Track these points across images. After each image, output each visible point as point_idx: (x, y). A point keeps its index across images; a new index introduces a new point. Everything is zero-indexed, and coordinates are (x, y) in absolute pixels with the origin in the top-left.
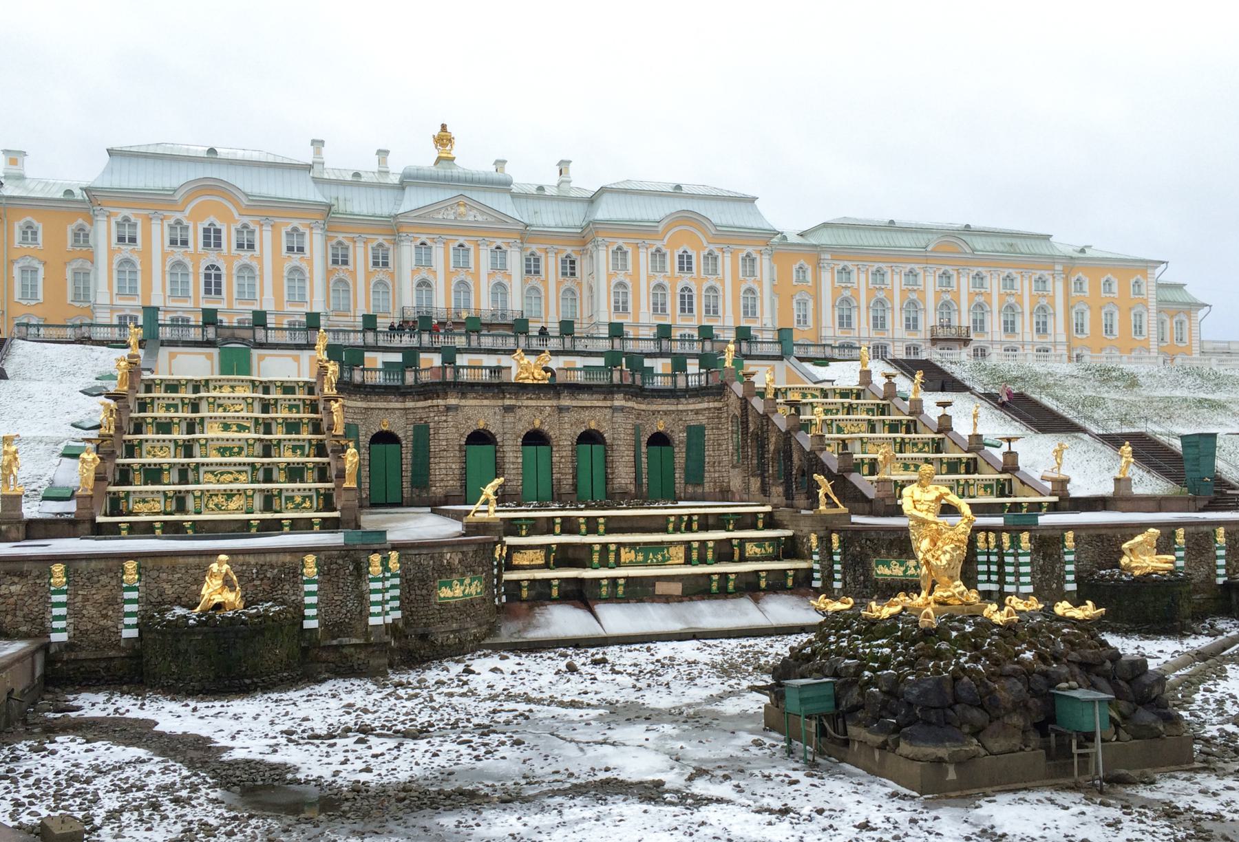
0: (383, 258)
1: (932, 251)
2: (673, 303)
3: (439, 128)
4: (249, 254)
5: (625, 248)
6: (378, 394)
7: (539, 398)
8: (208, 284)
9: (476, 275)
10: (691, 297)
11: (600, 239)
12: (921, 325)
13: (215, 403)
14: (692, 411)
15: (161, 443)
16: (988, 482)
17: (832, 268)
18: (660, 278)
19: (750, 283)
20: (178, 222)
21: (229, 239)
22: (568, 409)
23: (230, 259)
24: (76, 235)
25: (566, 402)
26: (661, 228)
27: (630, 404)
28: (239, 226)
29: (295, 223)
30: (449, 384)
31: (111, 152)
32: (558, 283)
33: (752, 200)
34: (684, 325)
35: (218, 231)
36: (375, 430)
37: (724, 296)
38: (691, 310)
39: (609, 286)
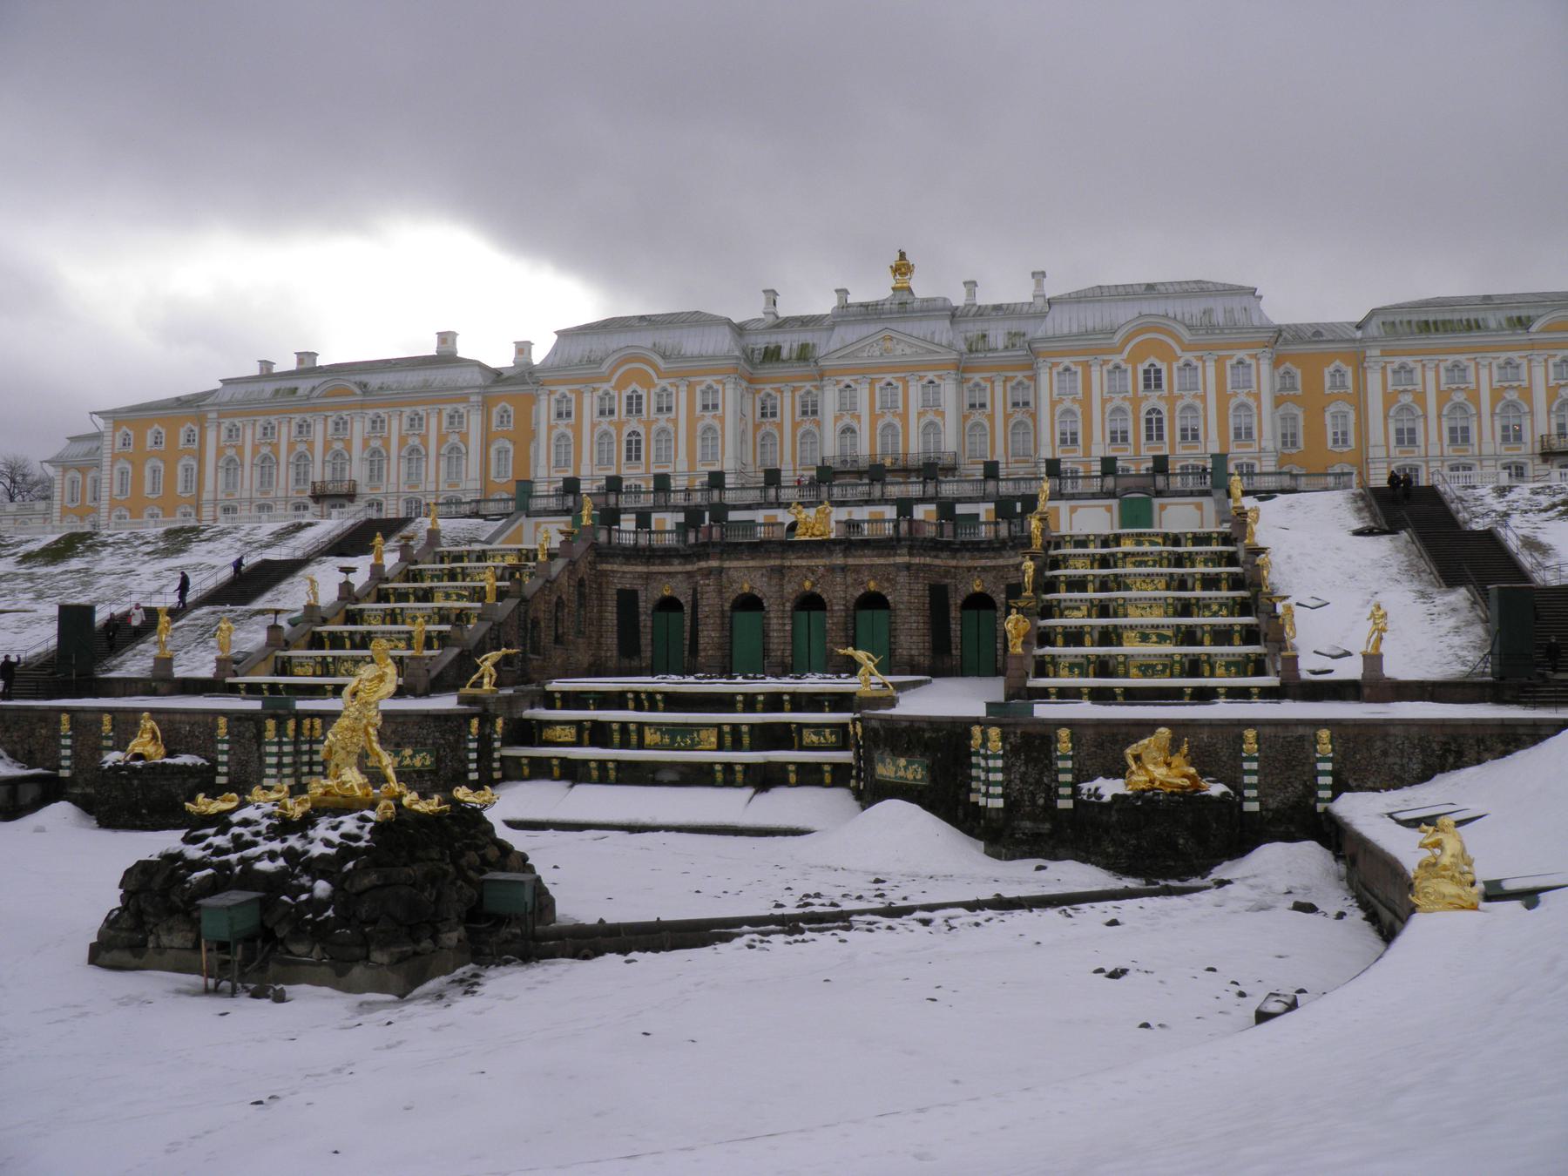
0: (812, 406)
1: (1537, 332)
2: (1136, 429)
3: (898, 259)
5: (1073, 368)
6: (660, 557)
7: (812, 557)
8: (629, 450)
9: (905, 417)
10: (1160, 421)
11: (1041, 360)
12: (1527, 436)
14: (1013, 566)
15: (374, 613)
16: (1231, 659)
17: (1384, 368)
18: (1117, 401)
19: (1242, 397)
20: (607, 393)
22: (844, 569)
23: (648, 424)
25: (839, 560)
26: (1117, 338)
27: (916, 560)
28: (658, 390)
29: (709, 380)
30: (714, 545)
31: (556, 332)
32: (1007, 417)
33: (1253, 291)
34: (637, 475)
35: (639, 397)
36: (657, 595)
37: (1206, 416)
38: (1160, 437)
39: (1052, 415)
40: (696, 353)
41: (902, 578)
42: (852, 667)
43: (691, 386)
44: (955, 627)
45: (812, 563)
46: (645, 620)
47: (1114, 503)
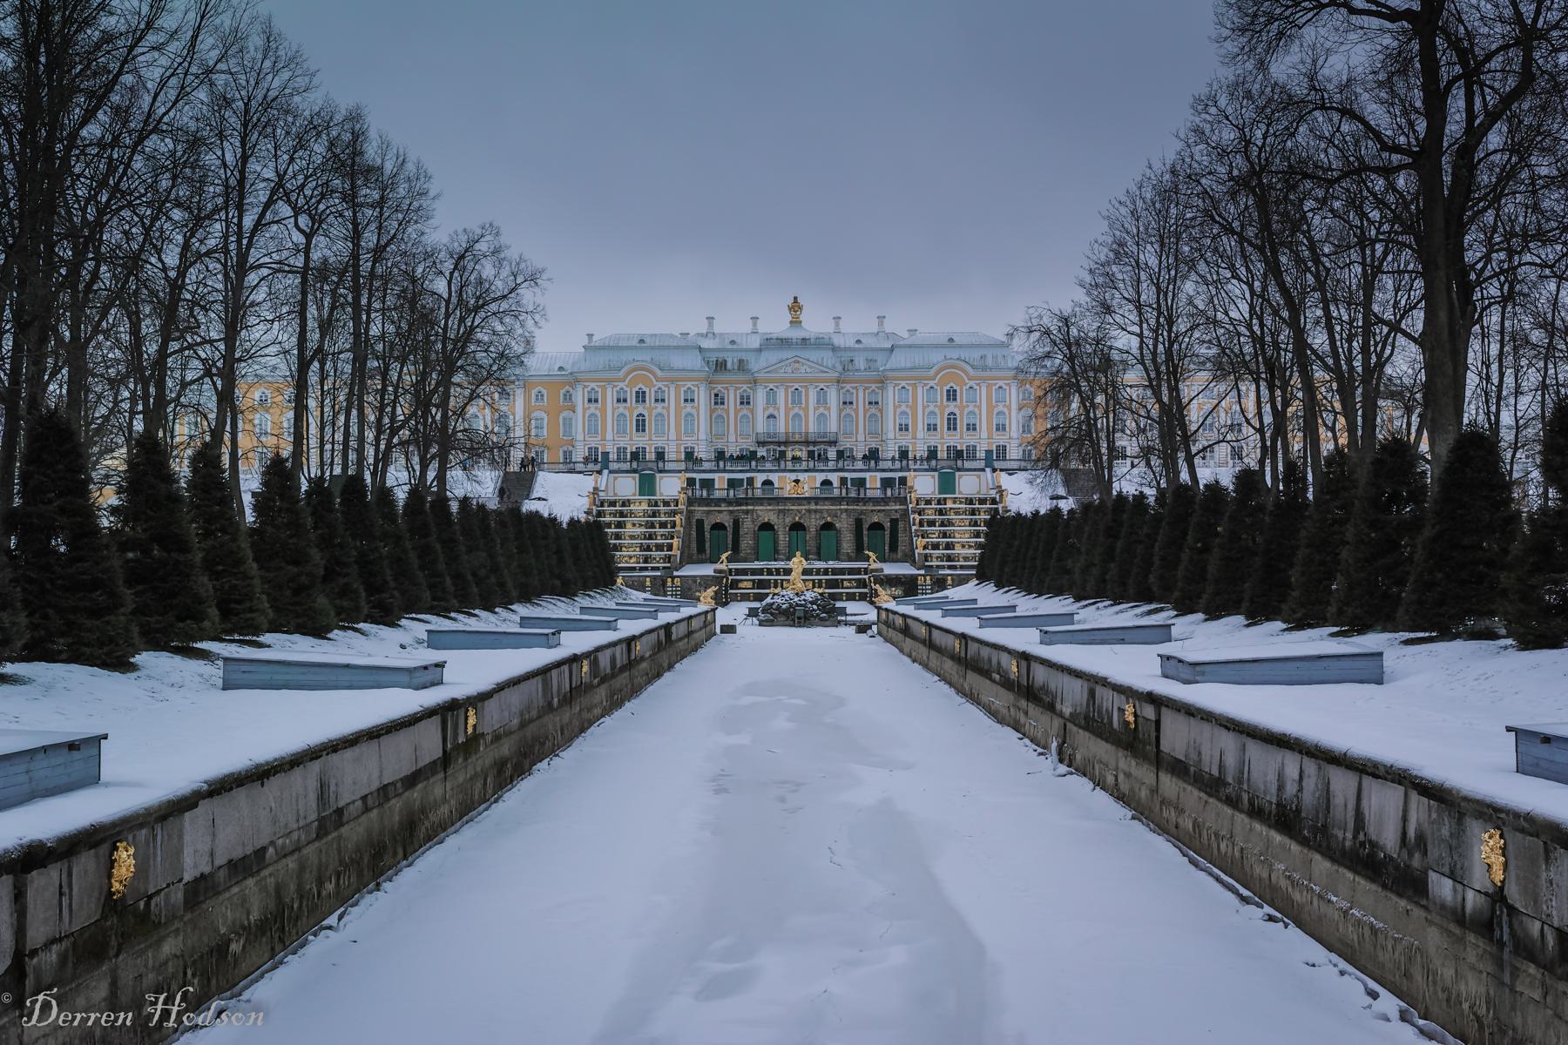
2: (942, 424)
4: (662, 404)
8: (638, 425)
13: (631, 513)
18: (932, 408)
19: (1001, 407)
21: (650, 397)
23: (650, 410)
24: (565, 395)
26: (932, 372)
28: (656, 388)
29: (689, 384)
32: (865, 411)
35: (644, 393)
38: (955, 429)
39: (895, 414)
40: (681, 367)
41: (844, 516)
42: (867, 559)
43: (677, 387)
44: (865, 539)
45: (800, 508)
46: (707, 535)
47: (936, 474)
